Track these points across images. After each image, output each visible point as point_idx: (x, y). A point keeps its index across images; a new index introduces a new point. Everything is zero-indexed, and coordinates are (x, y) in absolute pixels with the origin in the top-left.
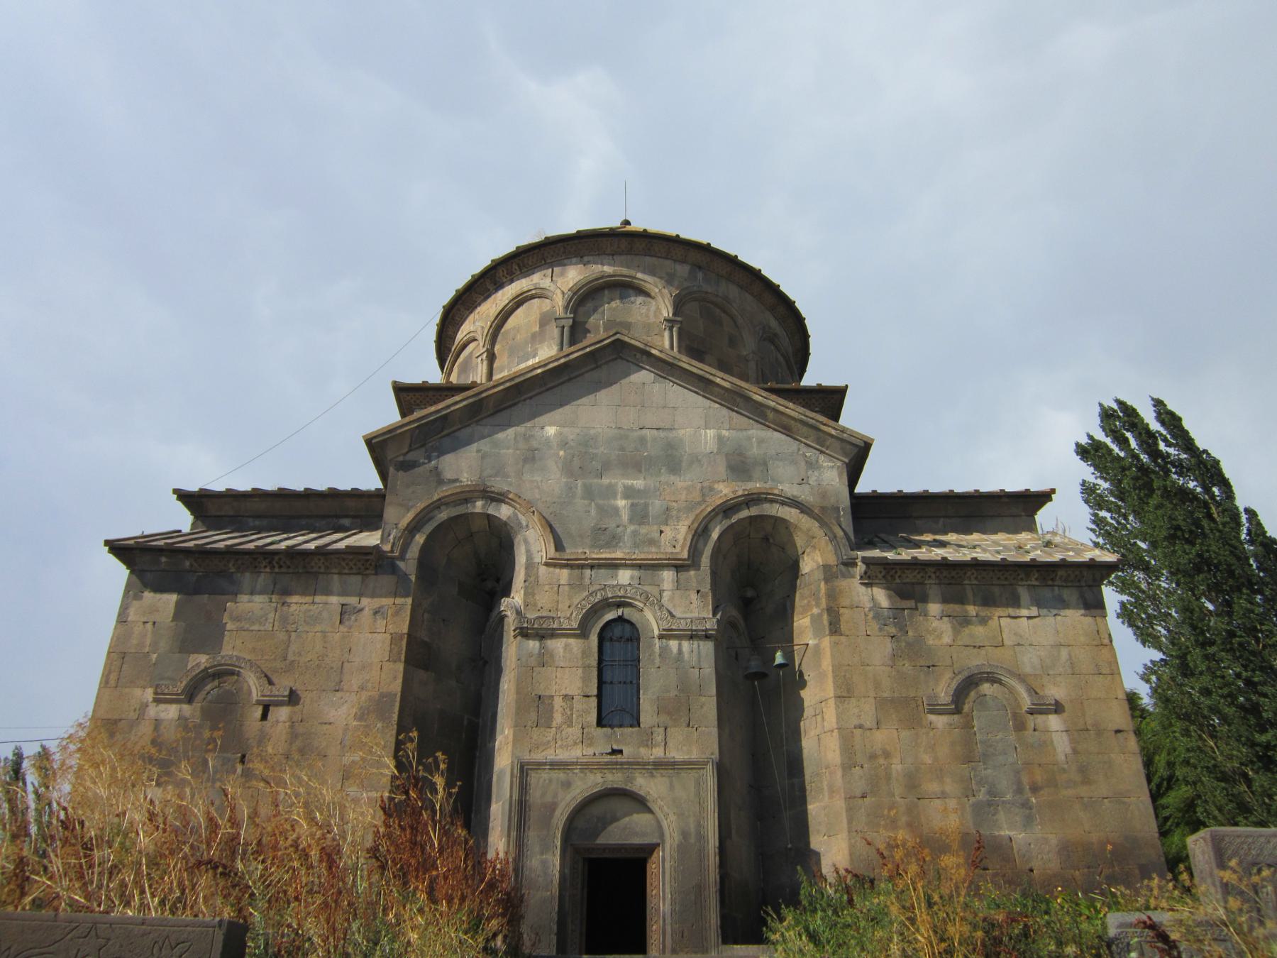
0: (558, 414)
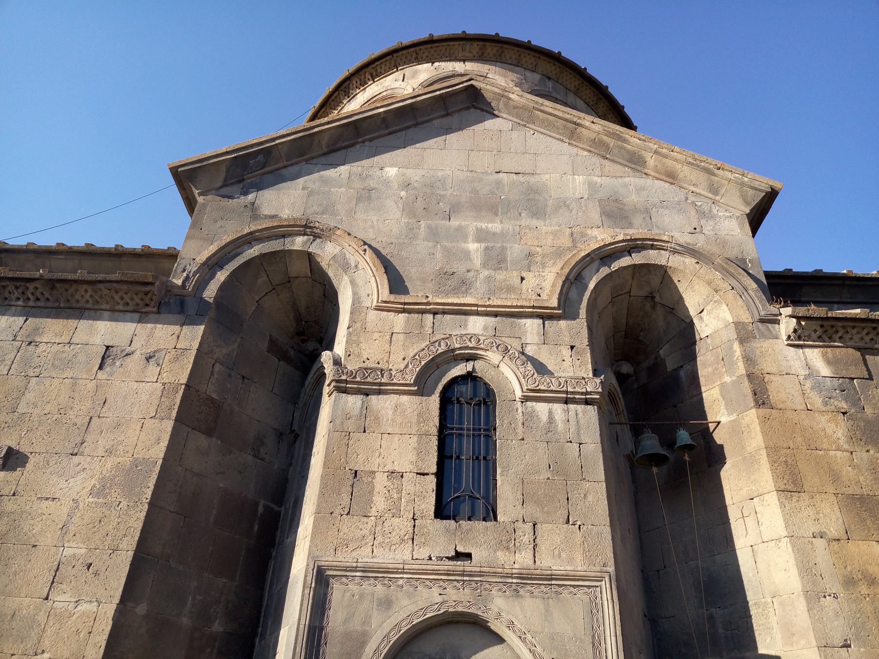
0: (399, 155)
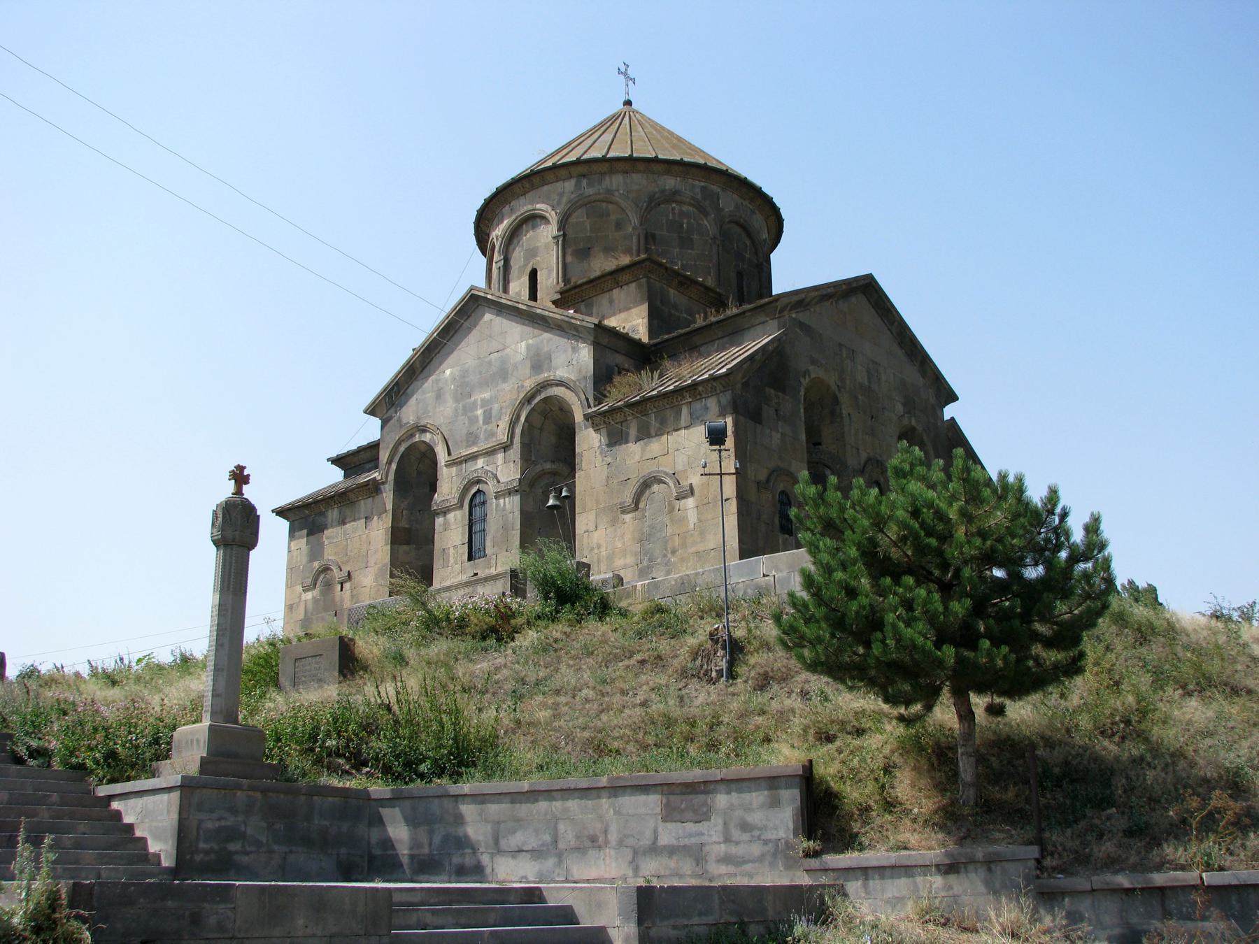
0: (451, 359)
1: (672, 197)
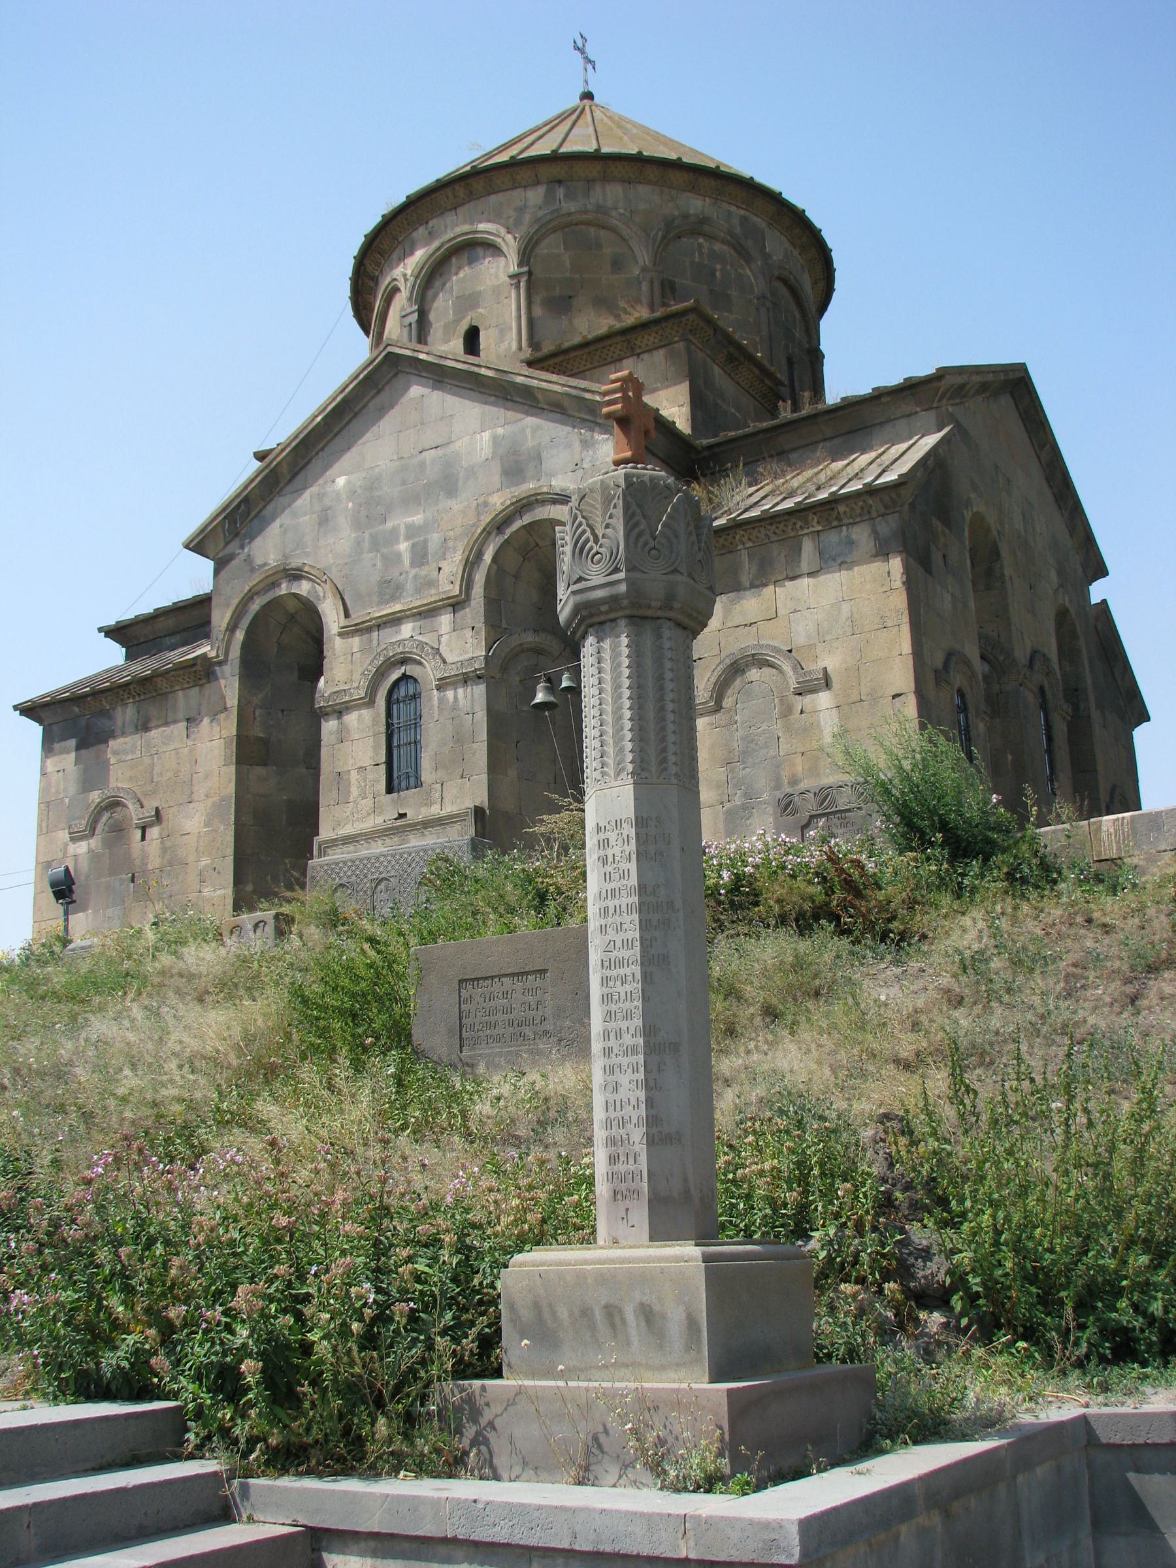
0: (348, 460)
1: (698, 227)
